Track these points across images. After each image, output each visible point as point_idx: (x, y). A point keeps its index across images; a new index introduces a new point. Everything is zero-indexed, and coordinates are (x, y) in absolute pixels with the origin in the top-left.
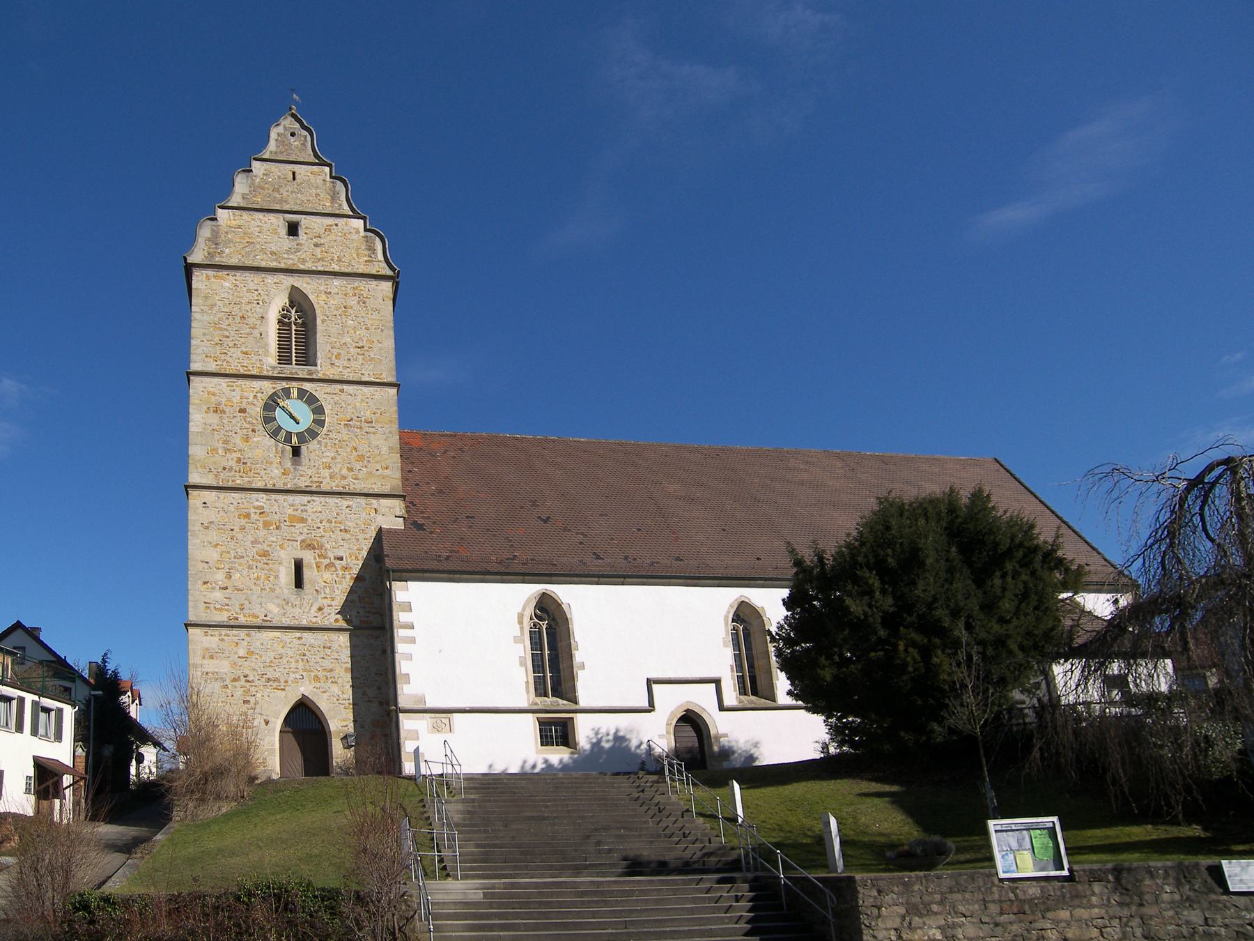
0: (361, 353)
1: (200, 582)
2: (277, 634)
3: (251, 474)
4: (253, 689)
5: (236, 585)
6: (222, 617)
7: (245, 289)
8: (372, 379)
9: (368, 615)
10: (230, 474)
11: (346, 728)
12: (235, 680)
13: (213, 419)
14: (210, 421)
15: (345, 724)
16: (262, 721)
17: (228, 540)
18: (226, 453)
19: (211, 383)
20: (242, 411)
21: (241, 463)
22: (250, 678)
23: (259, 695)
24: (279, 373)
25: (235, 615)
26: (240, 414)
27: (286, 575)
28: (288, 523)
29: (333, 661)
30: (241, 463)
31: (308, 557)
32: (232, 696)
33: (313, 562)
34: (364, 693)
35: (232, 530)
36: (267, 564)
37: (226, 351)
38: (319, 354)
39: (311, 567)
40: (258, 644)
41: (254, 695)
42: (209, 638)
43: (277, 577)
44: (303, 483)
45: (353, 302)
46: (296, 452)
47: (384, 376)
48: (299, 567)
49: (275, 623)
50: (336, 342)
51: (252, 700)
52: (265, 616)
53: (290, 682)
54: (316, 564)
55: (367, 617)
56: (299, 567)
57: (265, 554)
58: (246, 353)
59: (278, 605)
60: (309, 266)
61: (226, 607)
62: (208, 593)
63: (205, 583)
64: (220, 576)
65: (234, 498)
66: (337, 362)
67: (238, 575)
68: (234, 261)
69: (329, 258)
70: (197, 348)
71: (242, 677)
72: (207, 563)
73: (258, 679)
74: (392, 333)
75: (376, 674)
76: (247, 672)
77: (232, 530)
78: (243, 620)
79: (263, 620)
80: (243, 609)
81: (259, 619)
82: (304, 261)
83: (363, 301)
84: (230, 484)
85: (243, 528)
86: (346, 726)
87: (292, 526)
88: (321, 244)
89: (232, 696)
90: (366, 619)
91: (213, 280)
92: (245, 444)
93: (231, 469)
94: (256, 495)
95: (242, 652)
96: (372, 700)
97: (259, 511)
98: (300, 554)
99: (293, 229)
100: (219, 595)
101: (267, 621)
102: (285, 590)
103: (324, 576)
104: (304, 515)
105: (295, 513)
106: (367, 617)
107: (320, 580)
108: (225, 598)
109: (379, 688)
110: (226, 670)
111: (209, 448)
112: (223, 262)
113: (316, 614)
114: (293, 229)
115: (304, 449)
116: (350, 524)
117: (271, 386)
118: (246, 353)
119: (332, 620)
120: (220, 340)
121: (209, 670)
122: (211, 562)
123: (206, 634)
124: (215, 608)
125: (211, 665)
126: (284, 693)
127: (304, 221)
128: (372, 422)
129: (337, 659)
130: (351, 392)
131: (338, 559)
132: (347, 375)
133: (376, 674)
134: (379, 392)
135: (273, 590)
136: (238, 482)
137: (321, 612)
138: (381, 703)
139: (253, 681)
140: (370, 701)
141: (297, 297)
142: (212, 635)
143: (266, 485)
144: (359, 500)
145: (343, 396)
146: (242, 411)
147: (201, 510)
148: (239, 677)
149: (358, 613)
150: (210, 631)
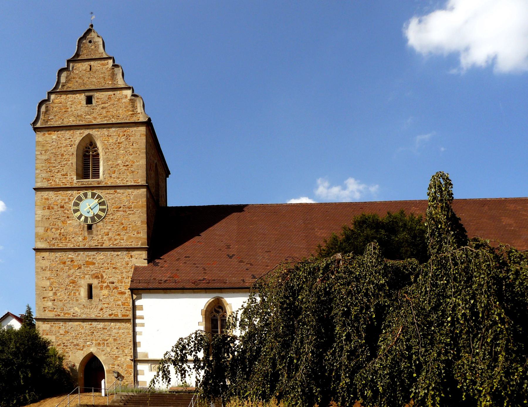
0: (127, 169)
6: (51, 315)
7: (63, 139)
8: (133, 184)
10: (56, 242)
11: (113, 369)
14: (45, 214)
20: (62, 207)
24: (82, 185)
26: (61, 209)
27: (83, 292)
28: (85, 266)
31: (95, 282)
44: (93, 244)
45: (123, 139)
46: (90, 227)
47: (139, 181)
48: (90, 287)
56: (90, 287)
57: (73, 282)
60: (98, 121)
62: (45, 303)
64: (51, 294)
66: (113, 175)
68: (58, 123)
70: (39, 175)
72: (44, 288)
74: (144, 155)
76: (64, 341)
79: (73, 316)
82: (95, 118)
83: (128, 138)
84: (56, 247)
86: (114, 368)
87: (87, 267)
93: (56, 239)
95: (62, 332)
98: (91, 281)
99: (89, 100)
101: (74, 316)
104: (94, 261)
105: (90, 260)
112: (52, 125)
113: (99, 312)
114: (89, 100)
115: (94, 226)
127: (96, 95)
128: (131, 208)
129: (110, 335)
131: (111, 283)
132: (119, 183)
134: (137, 192)
136: (60, 245)
143: (74, 246)
146: (62, 207)
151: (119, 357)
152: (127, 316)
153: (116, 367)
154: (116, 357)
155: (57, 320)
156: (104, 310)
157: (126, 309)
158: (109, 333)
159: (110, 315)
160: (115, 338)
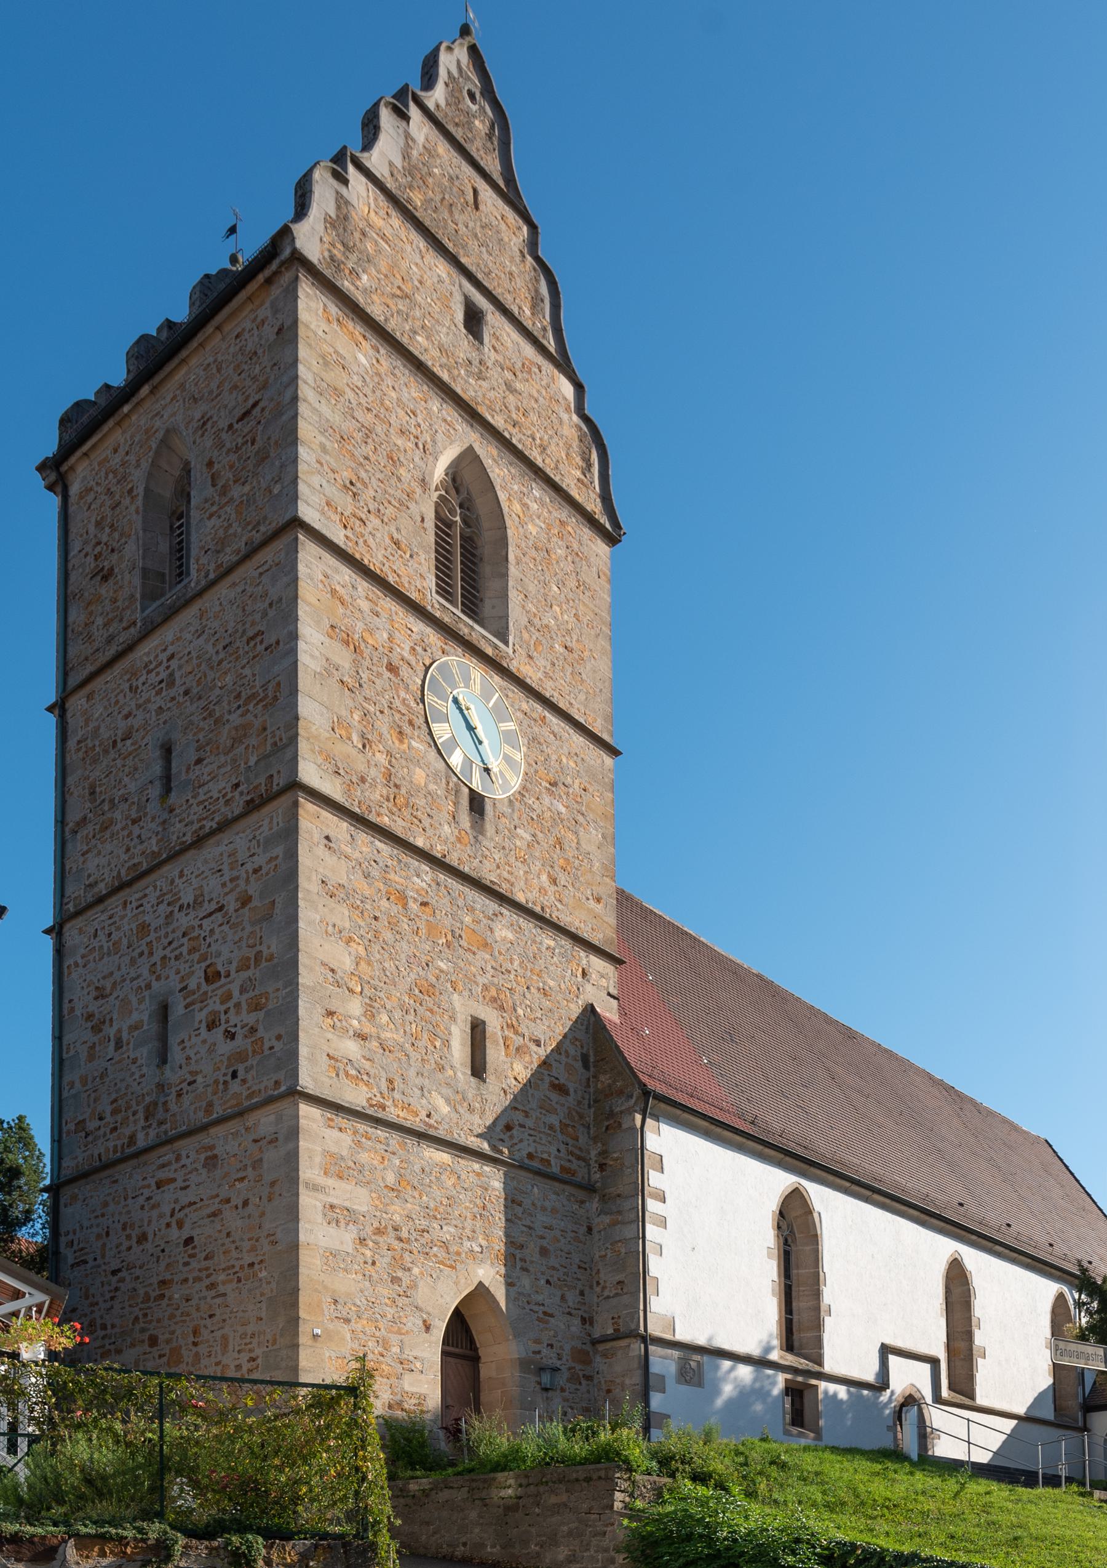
1: (320, 1010)
2: (444, 1157)
3: (406, 813)
4: (407, 1257)
5: (383, 1036)
6: (356, 1096)
9: (570, 1157)
11: (538, 1356)
12: (379, 1232)
13: (343, 658)
14: (336, 659)
15: (537, 1347)
16: (420, 1323)
17: (369, 936)
18: (364, 746)
19: (337, 571)
21: (391, 784)
22: (404, 1234)
23: (416, 1271)
25: (379, 1098)
29: (524, 1229)
30: (391, 784)
31: (494, 1022)
32: (374, 1263)
33: (499, 1033)
34: (563, 1297)
35: (376, 918)
36: (431, 1011)
37: (364, 517)
38: (511, 624)
39: (498, 1044)
40: (417, 1168)
41: (409, 1270)
42: (336, 1133)
43: (447, 1043)
49: (441, 1133)
50: (535, 615)
51: (406, 1280)
52: (429, 1116)
53: (463, 1255)
54: (505, 1039)
55: (569, 1161)
58: (397, 543)
59: (448, 1101)
61: (365, 1077)
63: (330, 1014)
64: (355, 1007)
65: (379, 852)
67: (384, 1018)
69: (529, 433)
70: (312, 473)
71: (390, 1229)
72: (333, 971)
73: (416, 1240)
75: (579, 1267)
77: (376, 918)
78: (393, 1113)
80: (393, 1090)
81: (418, 1119)
85: (393, 925)
86: (539, 1352)
88: (516, 390)
89: (374, 1263)
90: (567, 1164)
91: (335, 326)
92: (397, 742)
94: (417, 863)
96: (573, 1312)
97: (420, 900)
100: (351, 1048)
101: (431, 1126)
102: (459, 1074)
103: (515, 1066)
106: (569, 1161)
107: (510, 1074)
108: (364, 1057)
109: (582, 1293)
110: (364, 1209)
111: (336, 720)
113: (502, 1136)
116: (552, 983)
117: (439, 644)
118: (397, 543)
119: (524, 1153)
120: (351, 483)
121: (335, 1202)
122: (340, 973)
123: (331, 1123)
124: (347, 1074)
125: (344, 1193)
126: (453, 1273)
130: (556, 729)
133: (579, 1267)
135: (442, 1069)
137: (509, 1134)
138: (584, 1320)
139: (408, 1241)
140: (569, 1314)
141: (468, 476)
142: (340, 1130)
144: (563, 942)
145: (545, 731)
147: (321, 851)
148: (386, 1227)
149: (559, 1151)
150: (341, 1121)
151: (552, 1316)
152: (573, 1175)
153: (545, 1351)
154: (545, 1313)
155: (378, 1122)
156: (514, 1132)
157: (570, 1148)
158: (528, 1223)
159: (530, 1156)
160: (544, 1243)
